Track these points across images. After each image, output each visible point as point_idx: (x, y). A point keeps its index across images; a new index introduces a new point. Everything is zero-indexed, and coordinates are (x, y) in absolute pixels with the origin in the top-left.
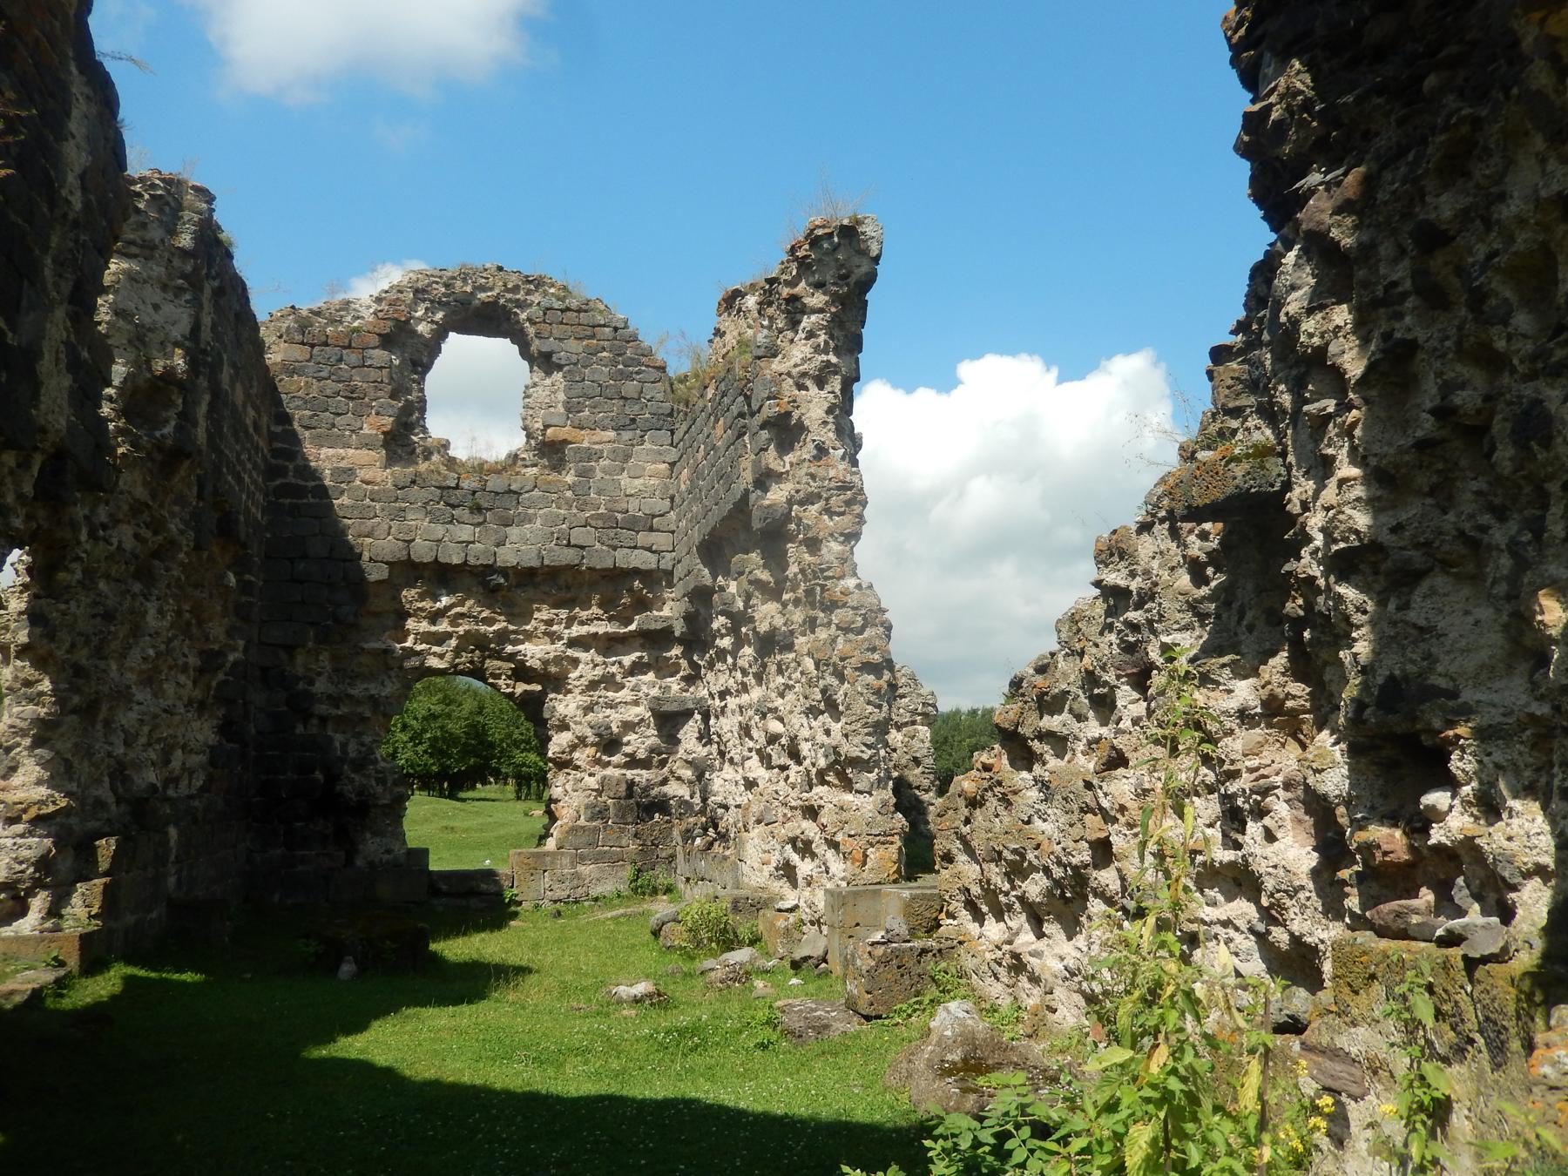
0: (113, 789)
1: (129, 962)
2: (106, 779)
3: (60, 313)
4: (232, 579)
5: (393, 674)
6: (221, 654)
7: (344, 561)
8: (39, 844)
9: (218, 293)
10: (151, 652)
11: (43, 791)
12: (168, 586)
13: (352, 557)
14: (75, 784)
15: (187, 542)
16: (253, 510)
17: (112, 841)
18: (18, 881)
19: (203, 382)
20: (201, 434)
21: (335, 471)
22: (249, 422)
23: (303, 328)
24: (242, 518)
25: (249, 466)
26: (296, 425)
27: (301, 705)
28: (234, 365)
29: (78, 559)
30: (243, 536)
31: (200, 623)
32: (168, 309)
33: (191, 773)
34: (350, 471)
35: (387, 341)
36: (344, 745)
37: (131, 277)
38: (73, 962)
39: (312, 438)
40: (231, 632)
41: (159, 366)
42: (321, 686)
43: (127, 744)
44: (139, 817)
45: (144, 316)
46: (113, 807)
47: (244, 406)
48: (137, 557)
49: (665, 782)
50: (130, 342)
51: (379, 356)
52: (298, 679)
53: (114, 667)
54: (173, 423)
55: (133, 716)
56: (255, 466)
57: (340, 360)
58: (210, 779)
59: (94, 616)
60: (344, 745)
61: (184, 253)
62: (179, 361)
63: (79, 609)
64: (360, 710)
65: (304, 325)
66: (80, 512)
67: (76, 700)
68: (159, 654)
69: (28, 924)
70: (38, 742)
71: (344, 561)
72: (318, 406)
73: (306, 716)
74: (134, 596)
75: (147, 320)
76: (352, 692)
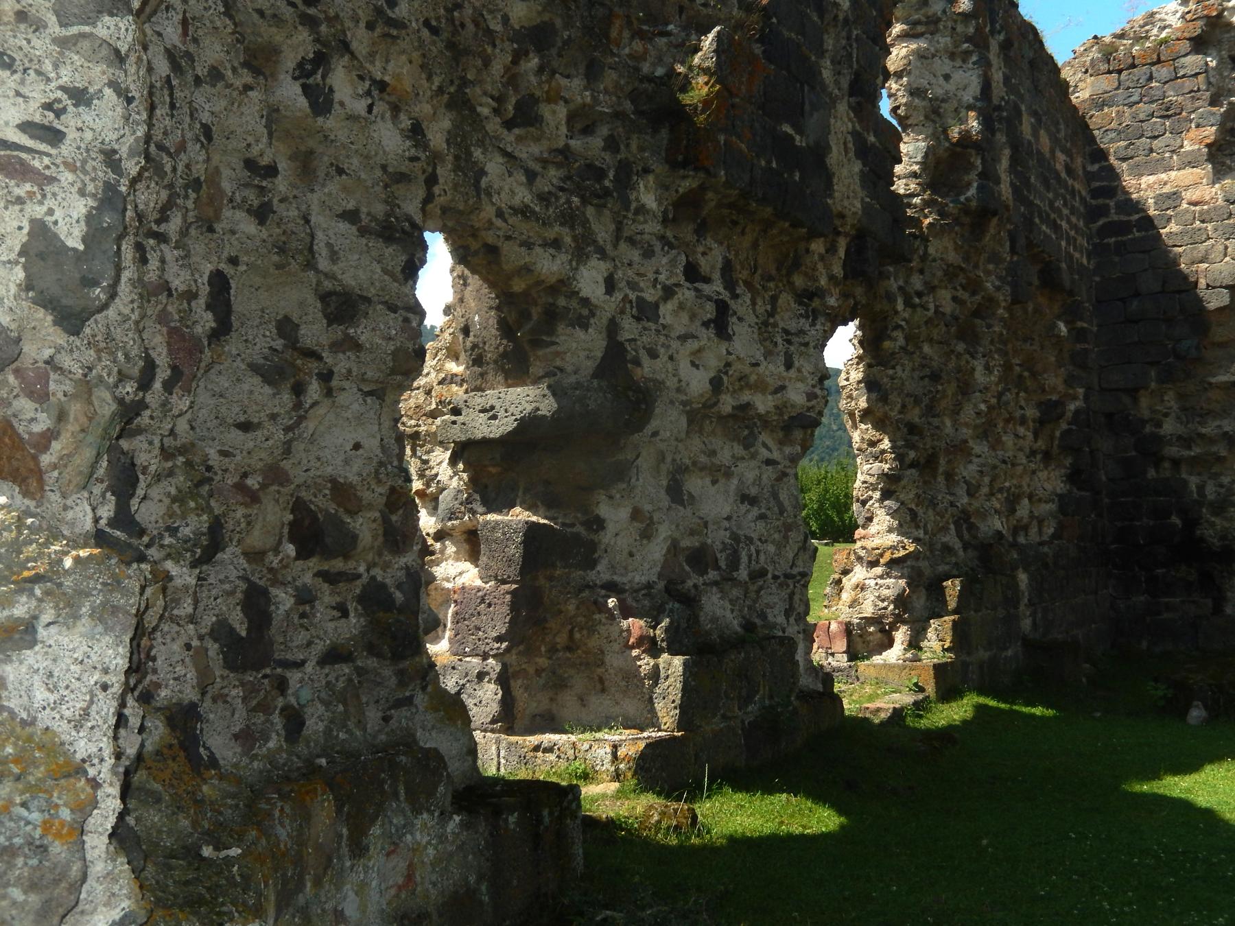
0: (960, 536)
1: (982, 692)
2: (952, 526)
3: (842, 107)
4: (1063, 328)
6: (1060, 404)
7: (1180, 292)
8: (895, 585)
9: (1006, 46)
10: (983, 407)
11: (893, 538)
12: (992, 342)
13: (1187, 286)
14: (922, 532)
15: (1003, 298)
16: (1077, 255)
17: (957, 582)
18: (882, 616)
19: (1001, 138)
20: (1005, 189)
21: (1160, 199)
22: (1059, 167)
23: (1109, 57)
24: (1064, 265)
25: (1066, 211)
26: (1112, 159)
27: (1151, 449)
28: (1035, 114)
29: (898, 327)
30: (1067, 284)
31: (1034, 375)
32: (958, 76)
33: (1041, 522)
34: (1175, 196)
35: (1199, 44)
36: (1201, 488)
37: (921, 55)
38: (931, 690)
39: (1131, 168)
40: (1070, 381)
41: (955, 133)
42: (1169, 427)
43: (970, 494)
44: (986, 563)
45: (938, 89)
46: (961, 553)
47: (1052, 152)
48: (956, 319)
50: (926, 117)
51: (1192, 62)
52: (1144, 422)
53: (948, 423)
54: (975, 185)
55: (973, 468)
56: (1073, 211)
57: (1151, 78)
58: (1061, 527)
59: (922, 378)
60: (1201, 488)
61: (965, 16)
62: (974, 124)
63: (904, 372)
64: (1214, 449)
65: (1108, 53)
66: (893, 285)
67: (912, 454)
68: (991, 408)
69: (895, 654)
70: (886, 495)
71: (1180, 292)
72: (1131, 134)
73: (1158, 460)
74: (959, 356)
75: (940, 92)
76: (1204, 431)
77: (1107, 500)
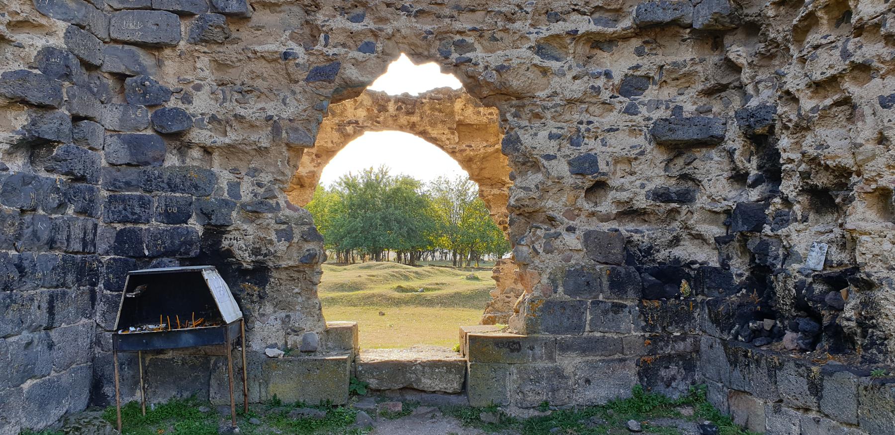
5: (297, 88)
36: (234, 188)
42: (202, 104)
49: (676, 241)
52: (167, 93)
60: (234, 188)
64: (254, 137)
73: (177, 139)
76: (242, 112)
77: (105, 193)
